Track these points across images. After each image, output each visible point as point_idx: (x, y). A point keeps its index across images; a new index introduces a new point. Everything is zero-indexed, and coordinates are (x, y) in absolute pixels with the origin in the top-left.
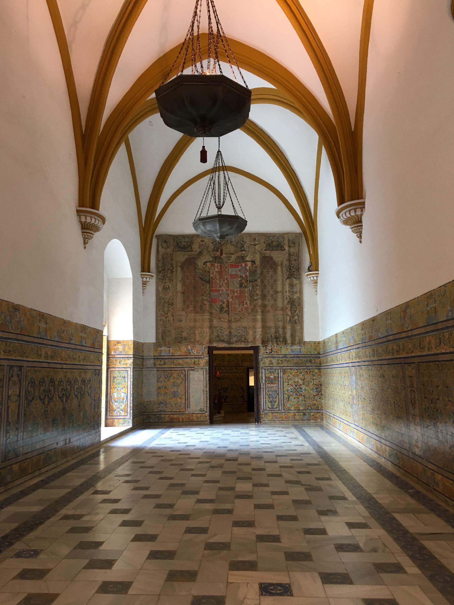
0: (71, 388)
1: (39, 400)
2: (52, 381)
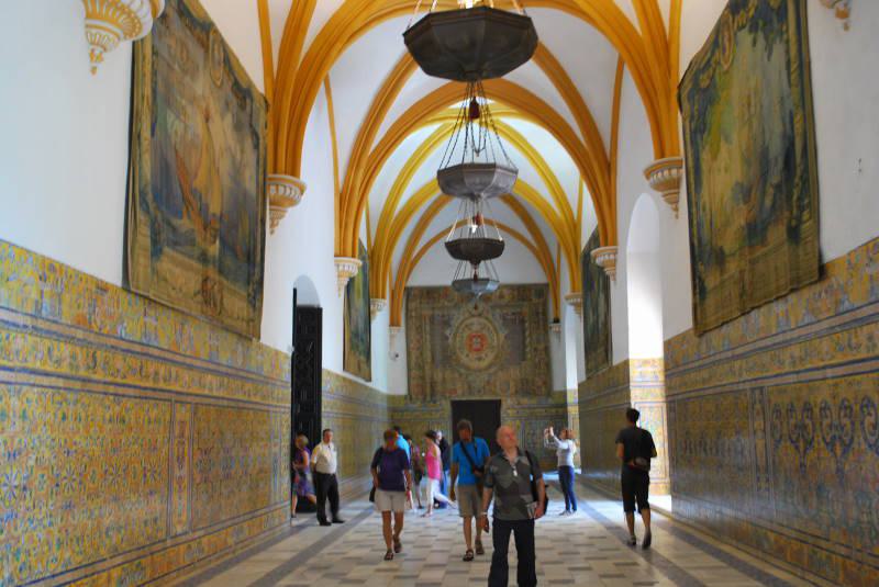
0: (853, 423)
1: (789, 443)
2: (808, 408)
